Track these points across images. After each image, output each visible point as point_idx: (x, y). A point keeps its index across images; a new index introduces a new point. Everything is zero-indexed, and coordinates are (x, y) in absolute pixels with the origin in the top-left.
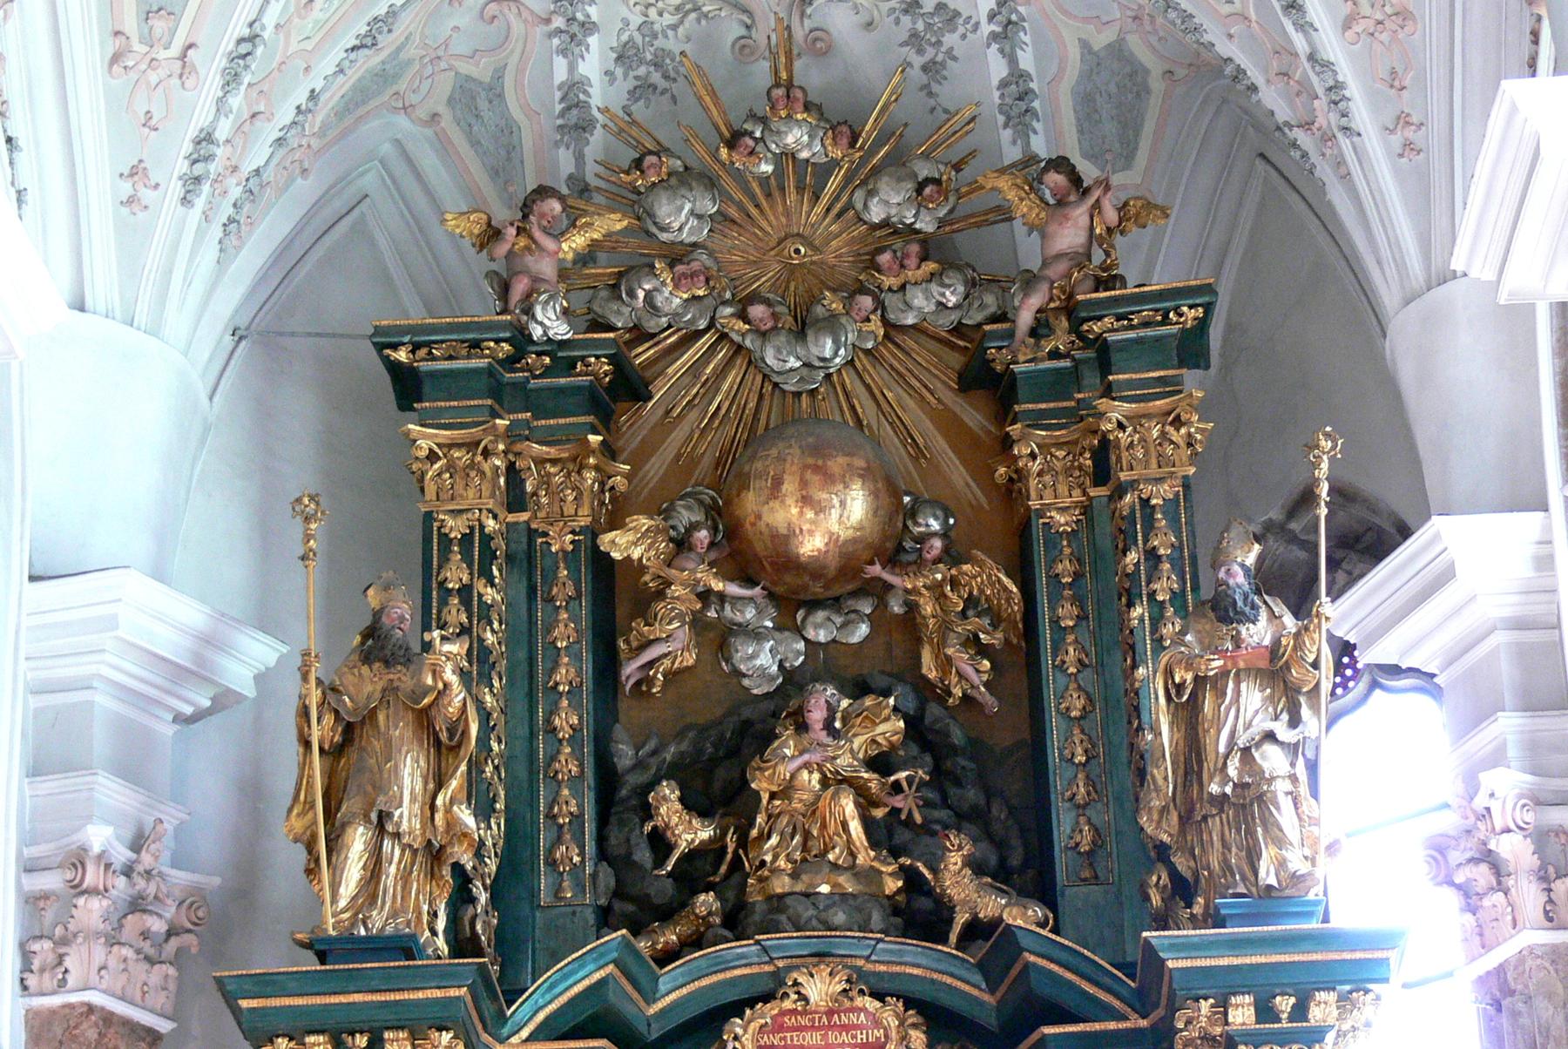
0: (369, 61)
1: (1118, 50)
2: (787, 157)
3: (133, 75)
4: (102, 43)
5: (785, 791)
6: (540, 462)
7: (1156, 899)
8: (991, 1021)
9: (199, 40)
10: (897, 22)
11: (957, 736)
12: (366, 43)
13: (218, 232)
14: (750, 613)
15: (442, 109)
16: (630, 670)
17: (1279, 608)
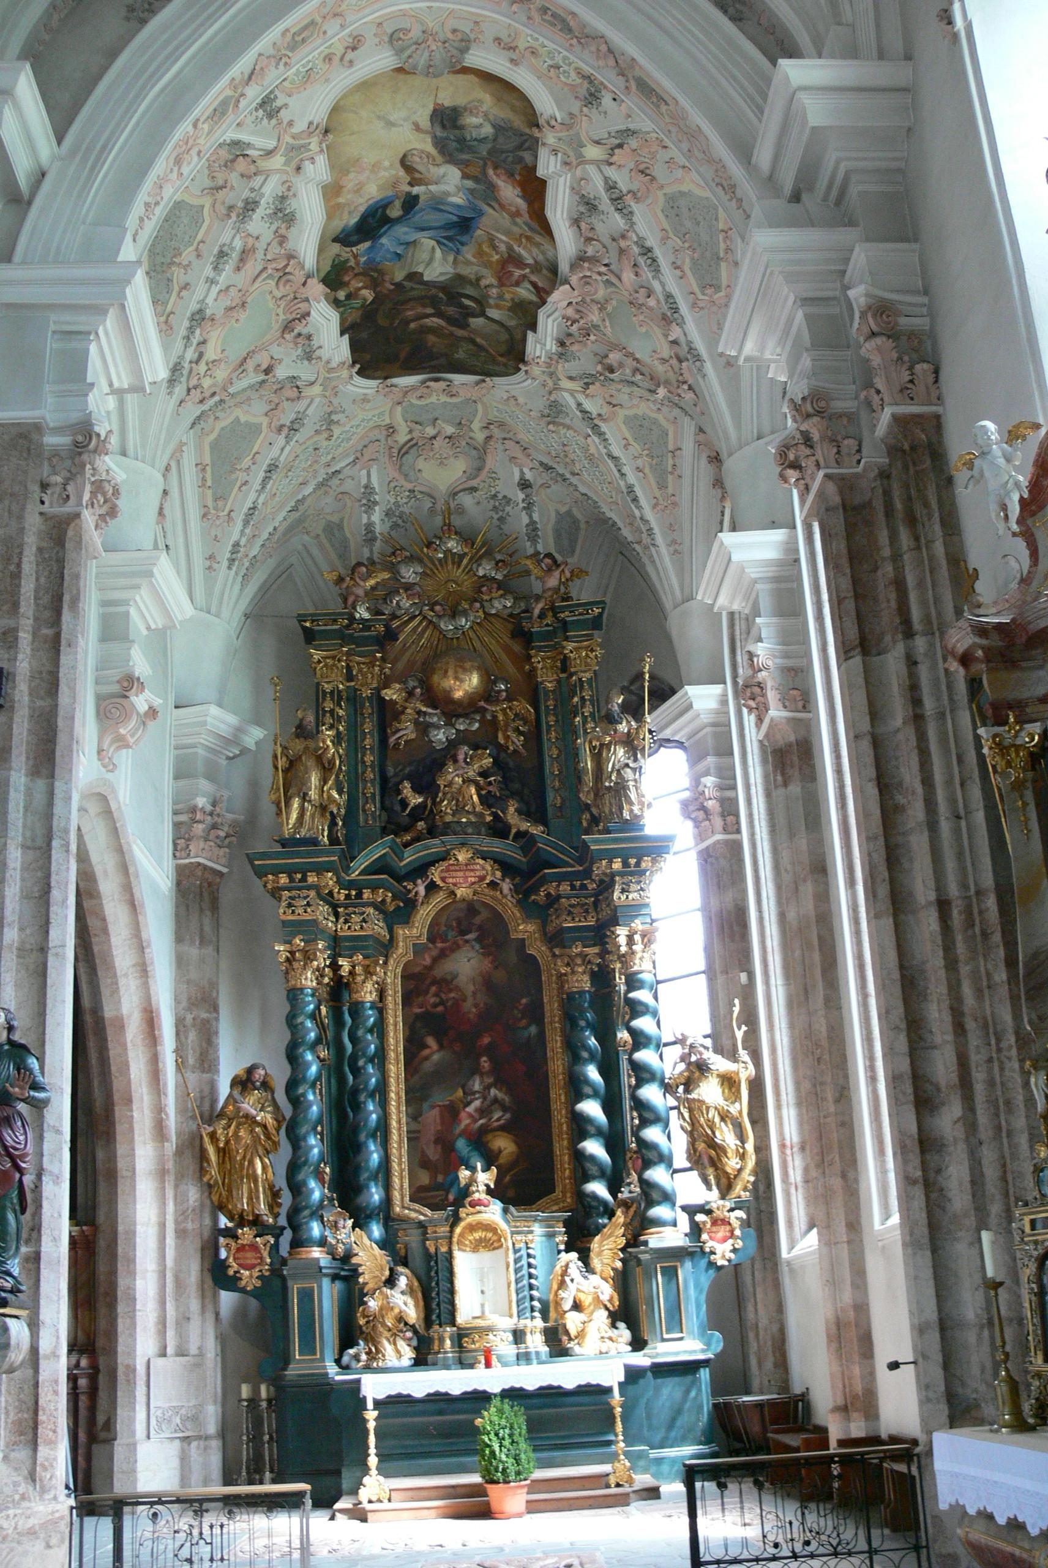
1: (569, 513)
2: (448, 552)
5: (450, 784)
6: (358, 663)
7: (585, 824)
8: (524, 867)
11: (511, 764)
13: (240, 579)
14: (435, 719)
15: (320, 532)
16: (392, 740)
17: (630, 718)
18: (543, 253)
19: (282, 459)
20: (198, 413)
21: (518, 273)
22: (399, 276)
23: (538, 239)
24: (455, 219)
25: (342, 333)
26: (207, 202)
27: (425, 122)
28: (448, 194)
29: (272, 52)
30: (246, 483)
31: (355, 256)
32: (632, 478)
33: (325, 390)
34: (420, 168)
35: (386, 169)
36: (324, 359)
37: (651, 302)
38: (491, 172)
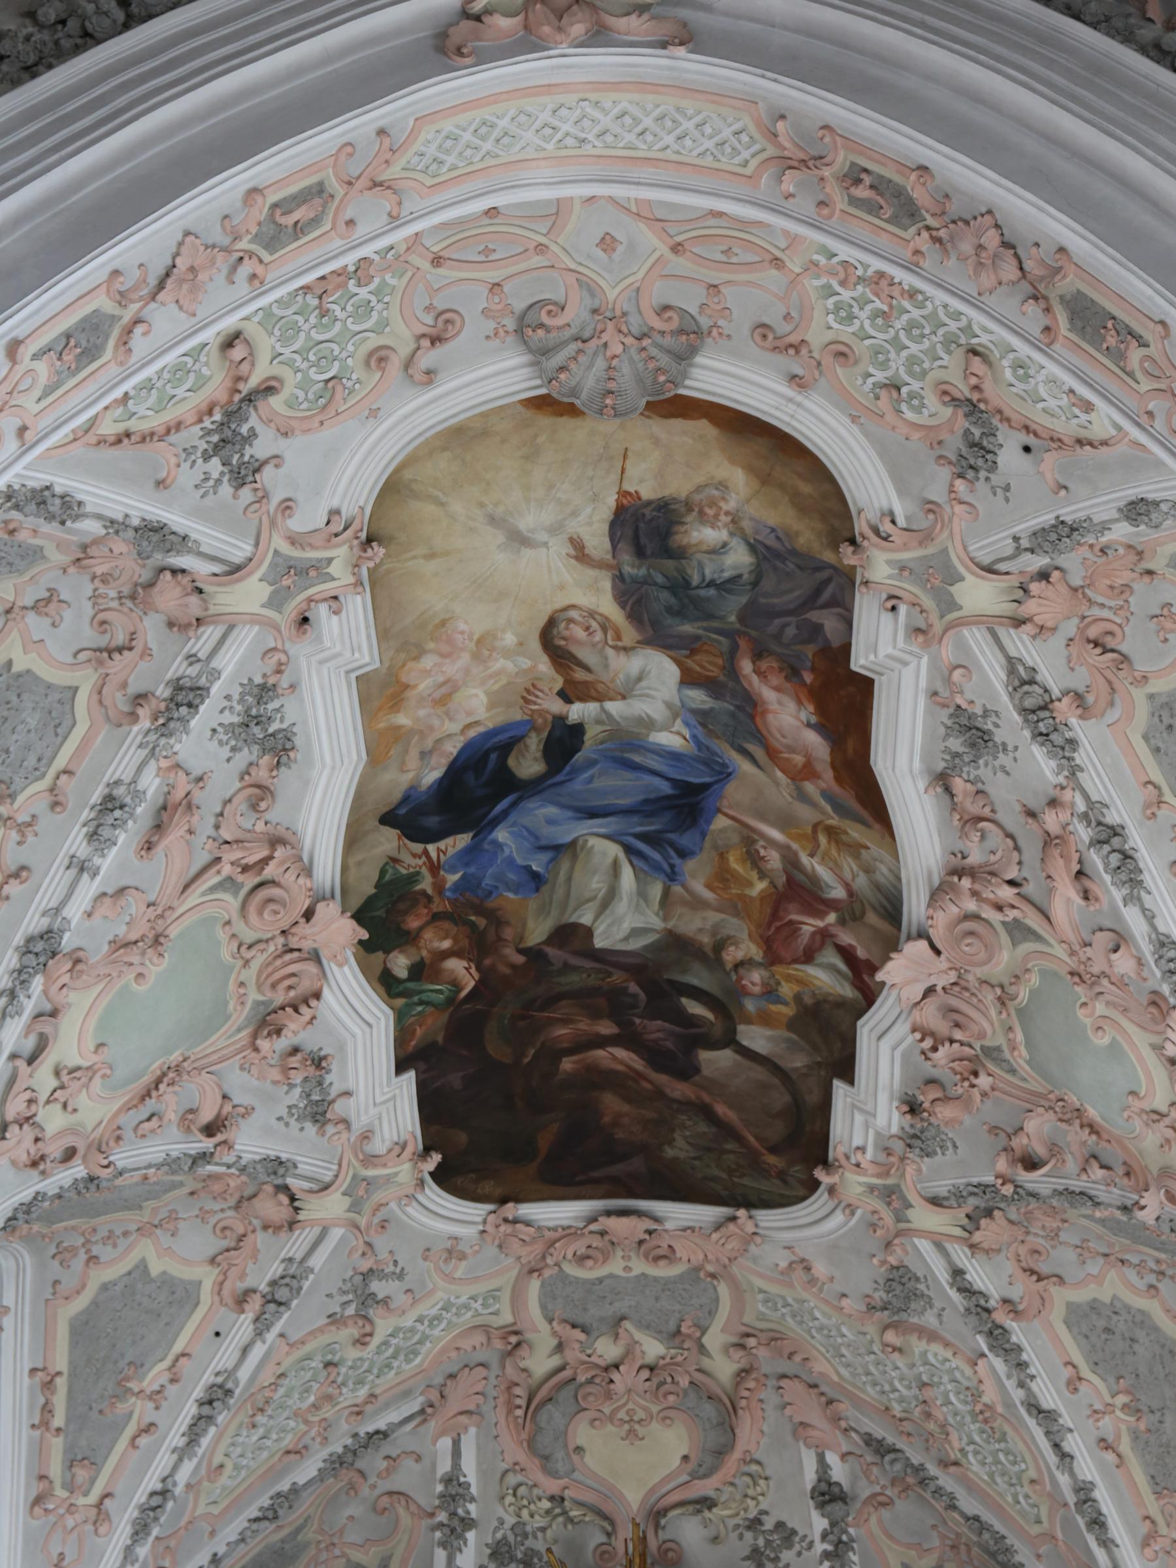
0: (270, 1534)
3: (52, 1518)
4: (28, 1486)
9: (118, 1490)
10: (741, 1537)
12: (269, 1515)
18: (868, 870)
19: (244, 1374)
20: (26, 1195)
21: (810, 925)
22: (537, 932)
23: (855, 832)
24: (666, 788)
25: (400, 1068)
26: (85, 680)
27: (598, 541)
28: (649, 724)
29: (218, 236)
30: (149, 1428)
31: (434, 868)
32: (1087, 1467)
33: (355, 1207)
34: (583, 654)
35: (507, 654)
36: (357, 1126)
37: (1123, 964)
38: (746, 666)
